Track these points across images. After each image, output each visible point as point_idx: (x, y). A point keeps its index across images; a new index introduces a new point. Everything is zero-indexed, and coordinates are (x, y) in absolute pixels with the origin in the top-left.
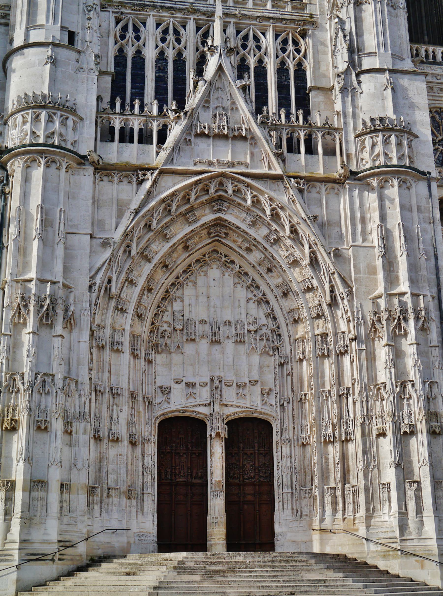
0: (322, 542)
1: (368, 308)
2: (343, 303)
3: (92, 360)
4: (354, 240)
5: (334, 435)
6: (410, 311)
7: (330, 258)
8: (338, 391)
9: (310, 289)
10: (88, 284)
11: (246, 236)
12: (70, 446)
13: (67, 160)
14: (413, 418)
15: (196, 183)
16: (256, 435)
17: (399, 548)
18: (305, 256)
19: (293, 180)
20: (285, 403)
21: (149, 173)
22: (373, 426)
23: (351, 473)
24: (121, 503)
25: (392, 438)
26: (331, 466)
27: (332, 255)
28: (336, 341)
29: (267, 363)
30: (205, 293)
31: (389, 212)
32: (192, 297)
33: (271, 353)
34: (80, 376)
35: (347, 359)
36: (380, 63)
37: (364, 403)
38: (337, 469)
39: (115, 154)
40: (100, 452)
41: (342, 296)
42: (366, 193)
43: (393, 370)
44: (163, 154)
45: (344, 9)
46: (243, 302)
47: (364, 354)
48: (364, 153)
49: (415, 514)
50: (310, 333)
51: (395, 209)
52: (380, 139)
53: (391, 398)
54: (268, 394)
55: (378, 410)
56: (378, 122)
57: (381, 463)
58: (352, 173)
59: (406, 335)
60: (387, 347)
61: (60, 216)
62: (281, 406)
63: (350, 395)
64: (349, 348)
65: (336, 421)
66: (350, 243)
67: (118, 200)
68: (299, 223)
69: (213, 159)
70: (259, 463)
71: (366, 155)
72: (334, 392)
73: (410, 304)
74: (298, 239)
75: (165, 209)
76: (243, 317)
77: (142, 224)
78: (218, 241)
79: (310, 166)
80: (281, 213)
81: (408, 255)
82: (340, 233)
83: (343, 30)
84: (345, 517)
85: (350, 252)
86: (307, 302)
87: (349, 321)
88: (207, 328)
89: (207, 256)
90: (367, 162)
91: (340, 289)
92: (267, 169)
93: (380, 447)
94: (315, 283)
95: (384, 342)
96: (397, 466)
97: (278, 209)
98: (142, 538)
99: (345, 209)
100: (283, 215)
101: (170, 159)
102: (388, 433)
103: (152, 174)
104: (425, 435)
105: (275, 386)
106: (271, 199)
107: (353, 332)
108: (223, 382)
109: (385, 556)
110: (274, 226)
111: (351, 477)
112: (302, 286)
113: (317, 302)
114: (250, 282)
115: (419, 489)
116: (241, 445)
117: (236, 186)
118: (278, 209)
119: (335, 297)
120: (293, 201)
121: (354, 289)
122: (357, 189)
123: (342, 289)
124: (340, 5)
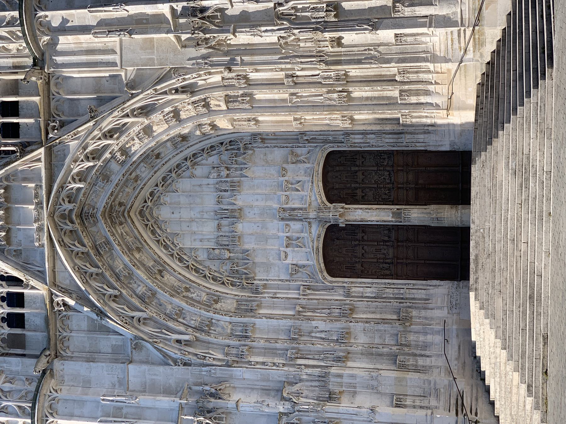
1: (192, 52)
2: (189, 79)
3: (263, 363)
5: (340, 92)
7: (138, 95)
8: (290, 87)
9: (176, 113)
10: (182, 367)
11: (121, 184)
12: (355, 393)
13: (49, 392)
14: (319, 6)
15: (63, 244)
16: (342, 168)
17: (471, 28)
19: (51, 135)
20: (305, 138)
21: (56, 300)
22: (328, 51)
23: (383, 73)
24: (415, 330)
25: (343, 33)
27: (134, 92)
28: (232, 86)
29: (262, 156)
30: (188, 224)
32: (193, 238)
33: (250, 152)
34: (280, 379)
37: (303, 60)
38: (379, 89)
39: (38, 333)
40: (362, 354)
41: (180, 80)
42: (59, 47)
43: (263, 29)
46: (195, 181)
47: (246, 58)
49: (432, 7)
53: (296, 31)
54: (297, 155)
55: (309, 44)
57: (372, 42)
58: (35, 64)
60: (237, 34)
61: (109, 400)
62: (309, 143)
63: (295, 74)
64: (240, 74)
65: (325, 90)
68: (100, 129)
69: (34, 226)
70: (373, 166)
71: (12, 47)
72: (292, 91)
74: (119, 128)
77: (114, 305)
78: (129, 212)
79: (33, 112)
80: (90, 148)
81: (127, 4)
82: (108, 79)
84: (434, 82)
86: (191, 117)
88: (225, 222)
89: (147, 223)
90: (21, 46)
92: (40, 164)
93: (353, 43)
95: (231, 36)
97: (85, 152)
98: (454, 303)
99: (79, 72)
100: (92, 146)
101: (40, 275)
103: (57, 296)
105: (287, 147)
106: (75, 161)
108: (285, 206)
109: (479, 44)
110: (107, 155)
112: (173, 122)
113: (190, 107)
114: (173, 175)
116: (353, 185)
117: (63, 200)
118: (85, 152)
119: (182, 87)
120: (75, 135)
122: (54, 58)
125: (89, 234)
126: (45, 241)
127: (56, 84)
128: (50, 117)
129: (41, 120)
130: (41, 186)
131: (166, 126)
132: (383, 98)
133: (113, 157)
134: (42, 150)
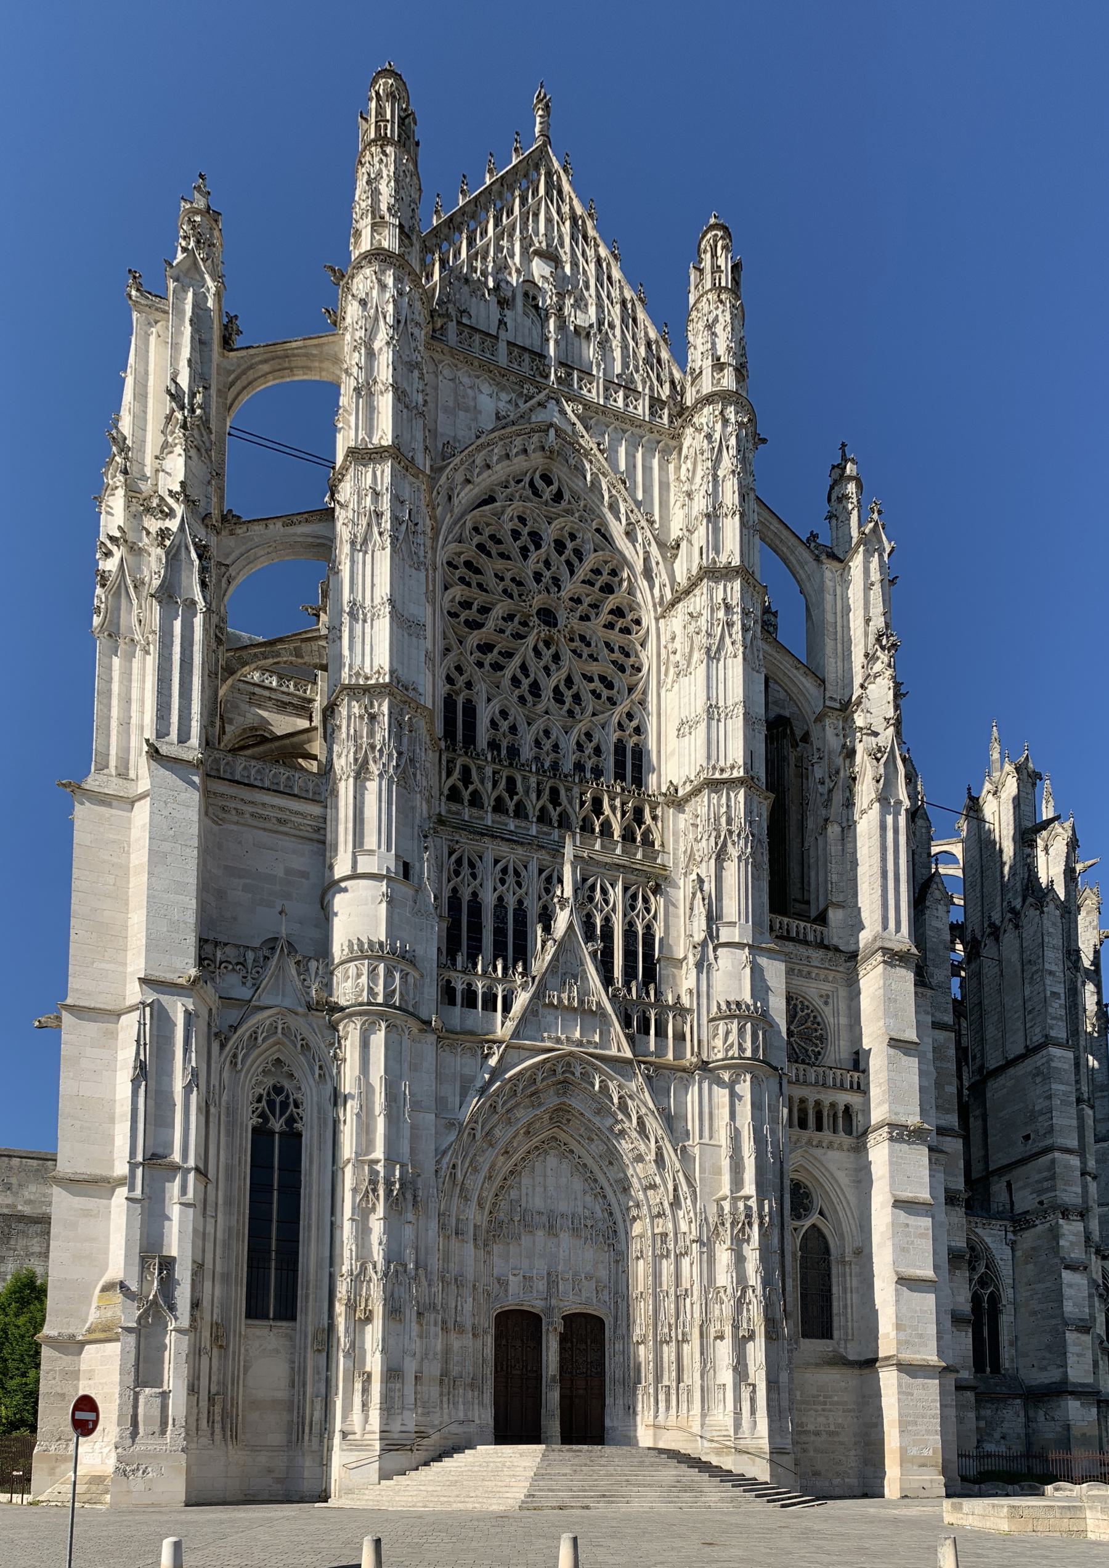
0: (656, 1438)
1: (713, 1209)
4: (701, 1137)
6: (755, 1215)
8: (676, 1292)
9: (653, 1187)
15: (544, 1061)
18: (650, 1151)
26: (666, 1365)
31: (738, 1108)
35: (685, 1262)
36: (740, 936)
42: (715, 1087)
43: (734, 1275)
44: (510, 1025)
45: (704, 864)
48: (716, 1040)
50: (649, 1232)
51: (745, 1104)
52: (734, 1027)
55: (717, 1313)
56: (733, 1007)
59: (748, 1241)
65: (673, 1321)
66: (697, 1140)
67: (461, 1075)
71: (718, 1042)
72: (672, 1291)
73: (755, 1209)
74: (645, 1132)
75: (511, 1088)
76: (580, 1210)
77: (488, 1104)
80: (629, 1102)
83: (702, 890)
85: (697, 1150)
87: (691, 1222)
91: (684, 1187)
94: (658, 1180)
95: (725, 1247)
96: (735, 1369)
102: (726, 1336)
104: (763, 1340)
106: (619, 1086)
107: (694, 1233)
110: (620, 1116)
111: (685, 1377)
115: (754, 1391)
121: (698, 1190)
123: (685, 1188)
124: (699, 859)
125: (549, 1086)
126: (548, 1044)
127: (681, 1078)
128: (658, 1067)
129: (652, 1059)
130: (596, 1048)
131: (642, 1176)
132: (662, 1371)
133: (617, 1122)
134: (629, 1054)
